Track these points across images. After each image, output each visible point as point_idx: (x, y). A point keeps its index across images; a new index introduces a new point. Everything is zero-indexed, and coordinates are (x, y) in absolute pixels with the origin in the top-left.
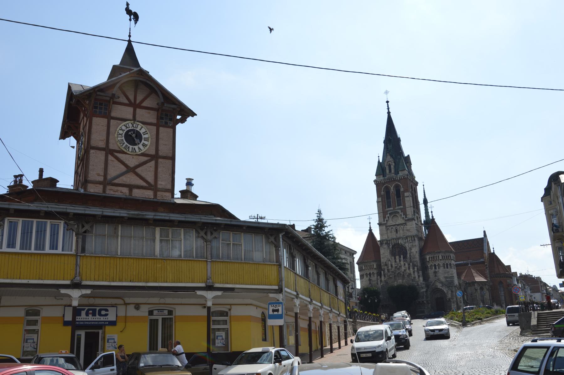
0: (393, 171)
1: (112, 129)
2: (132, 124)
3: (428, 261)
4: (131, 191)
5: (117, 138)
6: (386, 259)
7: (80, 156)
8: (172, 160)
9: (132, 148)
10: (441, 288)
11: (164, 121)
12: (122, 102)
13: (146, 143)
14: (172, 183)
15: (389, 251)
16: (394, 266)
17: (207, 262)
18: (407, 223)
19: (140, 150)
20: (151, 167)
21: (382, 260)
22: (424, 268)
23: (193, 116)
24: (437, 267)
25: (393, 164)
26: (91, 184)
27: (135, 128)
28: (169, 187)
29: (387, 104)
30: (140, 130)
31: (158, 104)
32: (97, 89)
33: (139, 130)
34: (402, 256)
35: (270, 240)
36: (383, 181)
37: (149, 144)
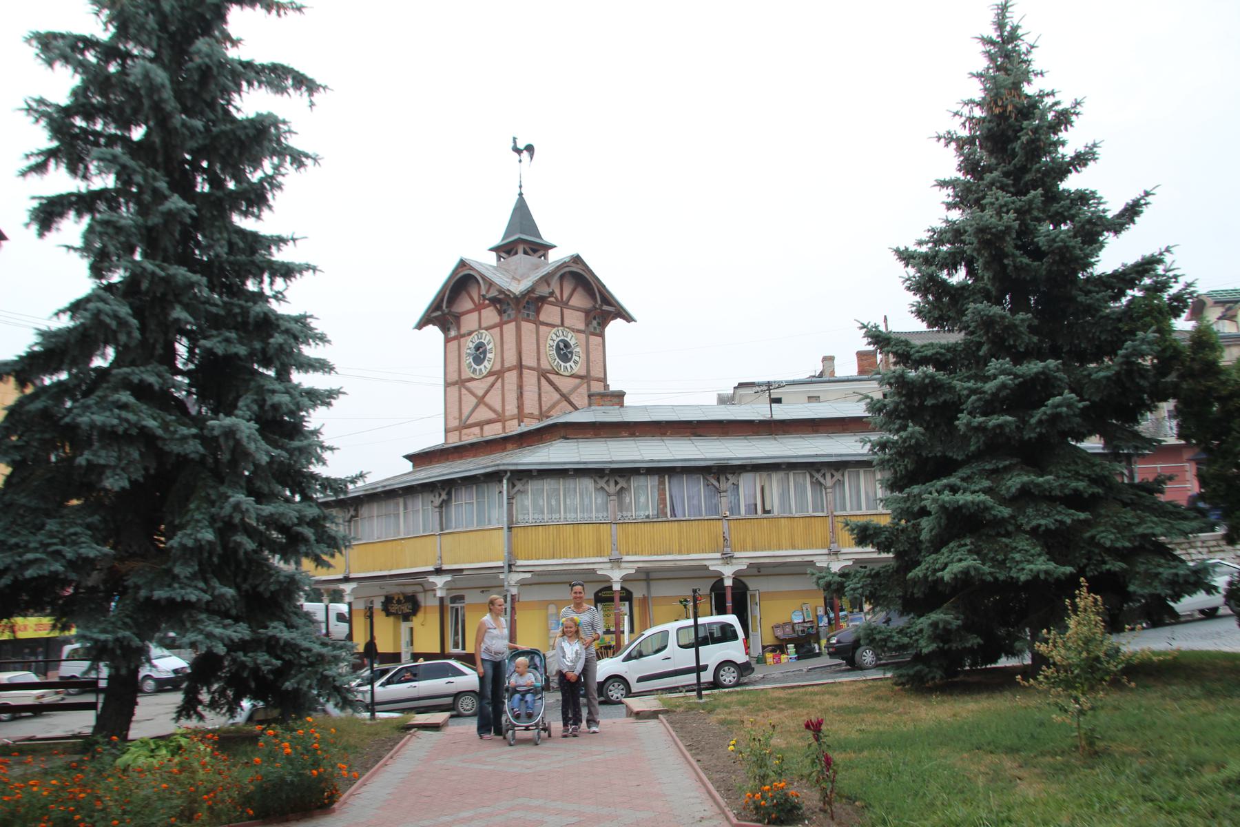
4: (482, 429)
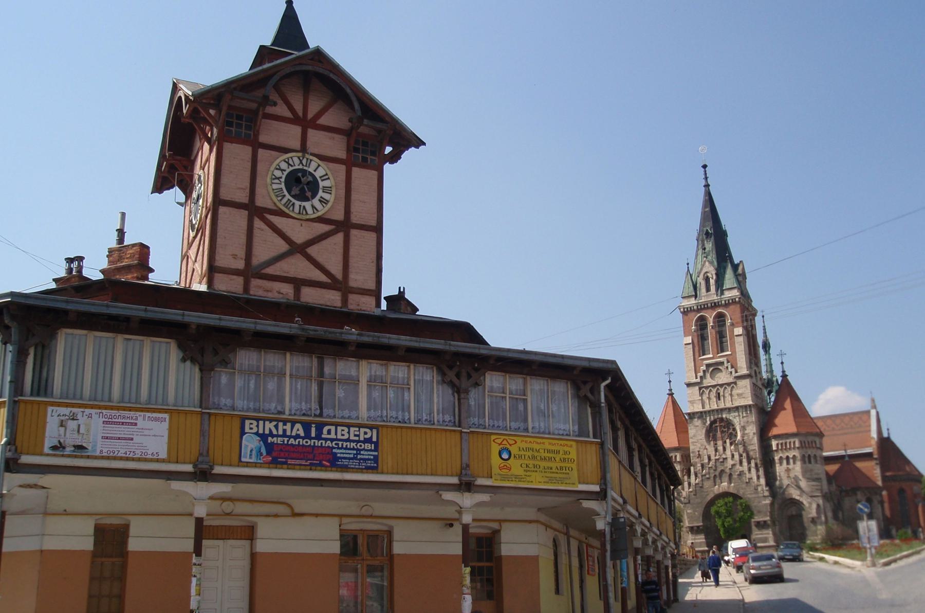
0: (713, 288)
1: (260, 167)
2: (299, 158)
3: (776, 451)
4: (297, 292)
5: (271, 185)
6: (699, 445)
7: (194, 222)
8: (376, 232)
9: (300, 206)
10: (798, 498)
11: (360, 155)
12: (279, 114)
13: (326, 196)
14: (376, 277)
15: (704, 431)
16: (713, 458)
17: (461, 434)
18: (737, 383)
19: (315, 211)
20: (335, 244)
21: (692, 447)
22: (767, 463)
23: (417, 147)
24: (791, 461)
25: (714, 277)
26: (220, 275)
27: (306, 166)
28: (372, 285)
29: (703, 169)
30: (315, 171)
31: (350, 121)
32: (233, 86)
33: (313, 172)
34: (728, 441)
35: (582, 393)
36: (695, 307)
37: (332, 200)
